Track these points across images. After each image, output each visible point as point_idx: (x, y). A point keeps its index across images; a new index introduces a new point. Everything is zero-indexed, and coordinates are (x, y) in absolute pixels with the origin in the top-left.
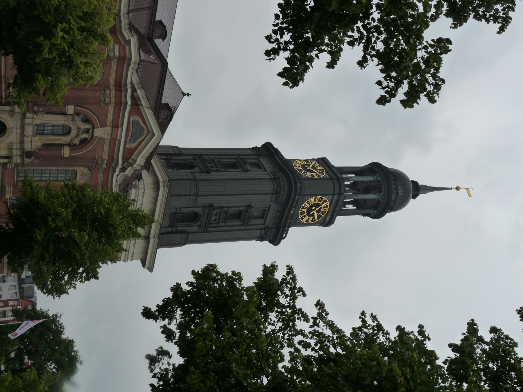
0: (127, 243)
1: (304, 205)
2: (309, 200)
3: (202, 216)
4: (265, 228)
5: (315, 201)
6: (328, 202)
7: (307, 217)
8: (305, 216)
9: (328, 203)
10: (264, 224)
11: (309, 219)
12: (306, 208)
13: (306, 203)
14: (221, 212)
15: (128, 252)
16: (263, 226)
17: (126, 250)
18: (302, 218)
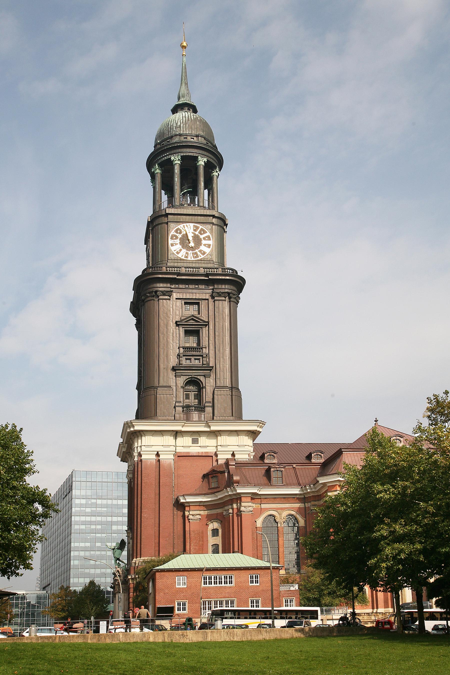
0: (220, 454)
1: (182, 256)
2: (175, 252)
3: (191, 376)
4: (213, 297)
5: (176, 244)
6: (179, 227)
7: (202, 248)
8: (200, 251)
9: (181, 226)
10: (208, 299)
11: (205, 245)
12: (187, 253)
13: (180, 255)
14: (184, 356)
15: (234, 452)
16: (211, 300)
17: (233, 455)
18: (204, 253)
